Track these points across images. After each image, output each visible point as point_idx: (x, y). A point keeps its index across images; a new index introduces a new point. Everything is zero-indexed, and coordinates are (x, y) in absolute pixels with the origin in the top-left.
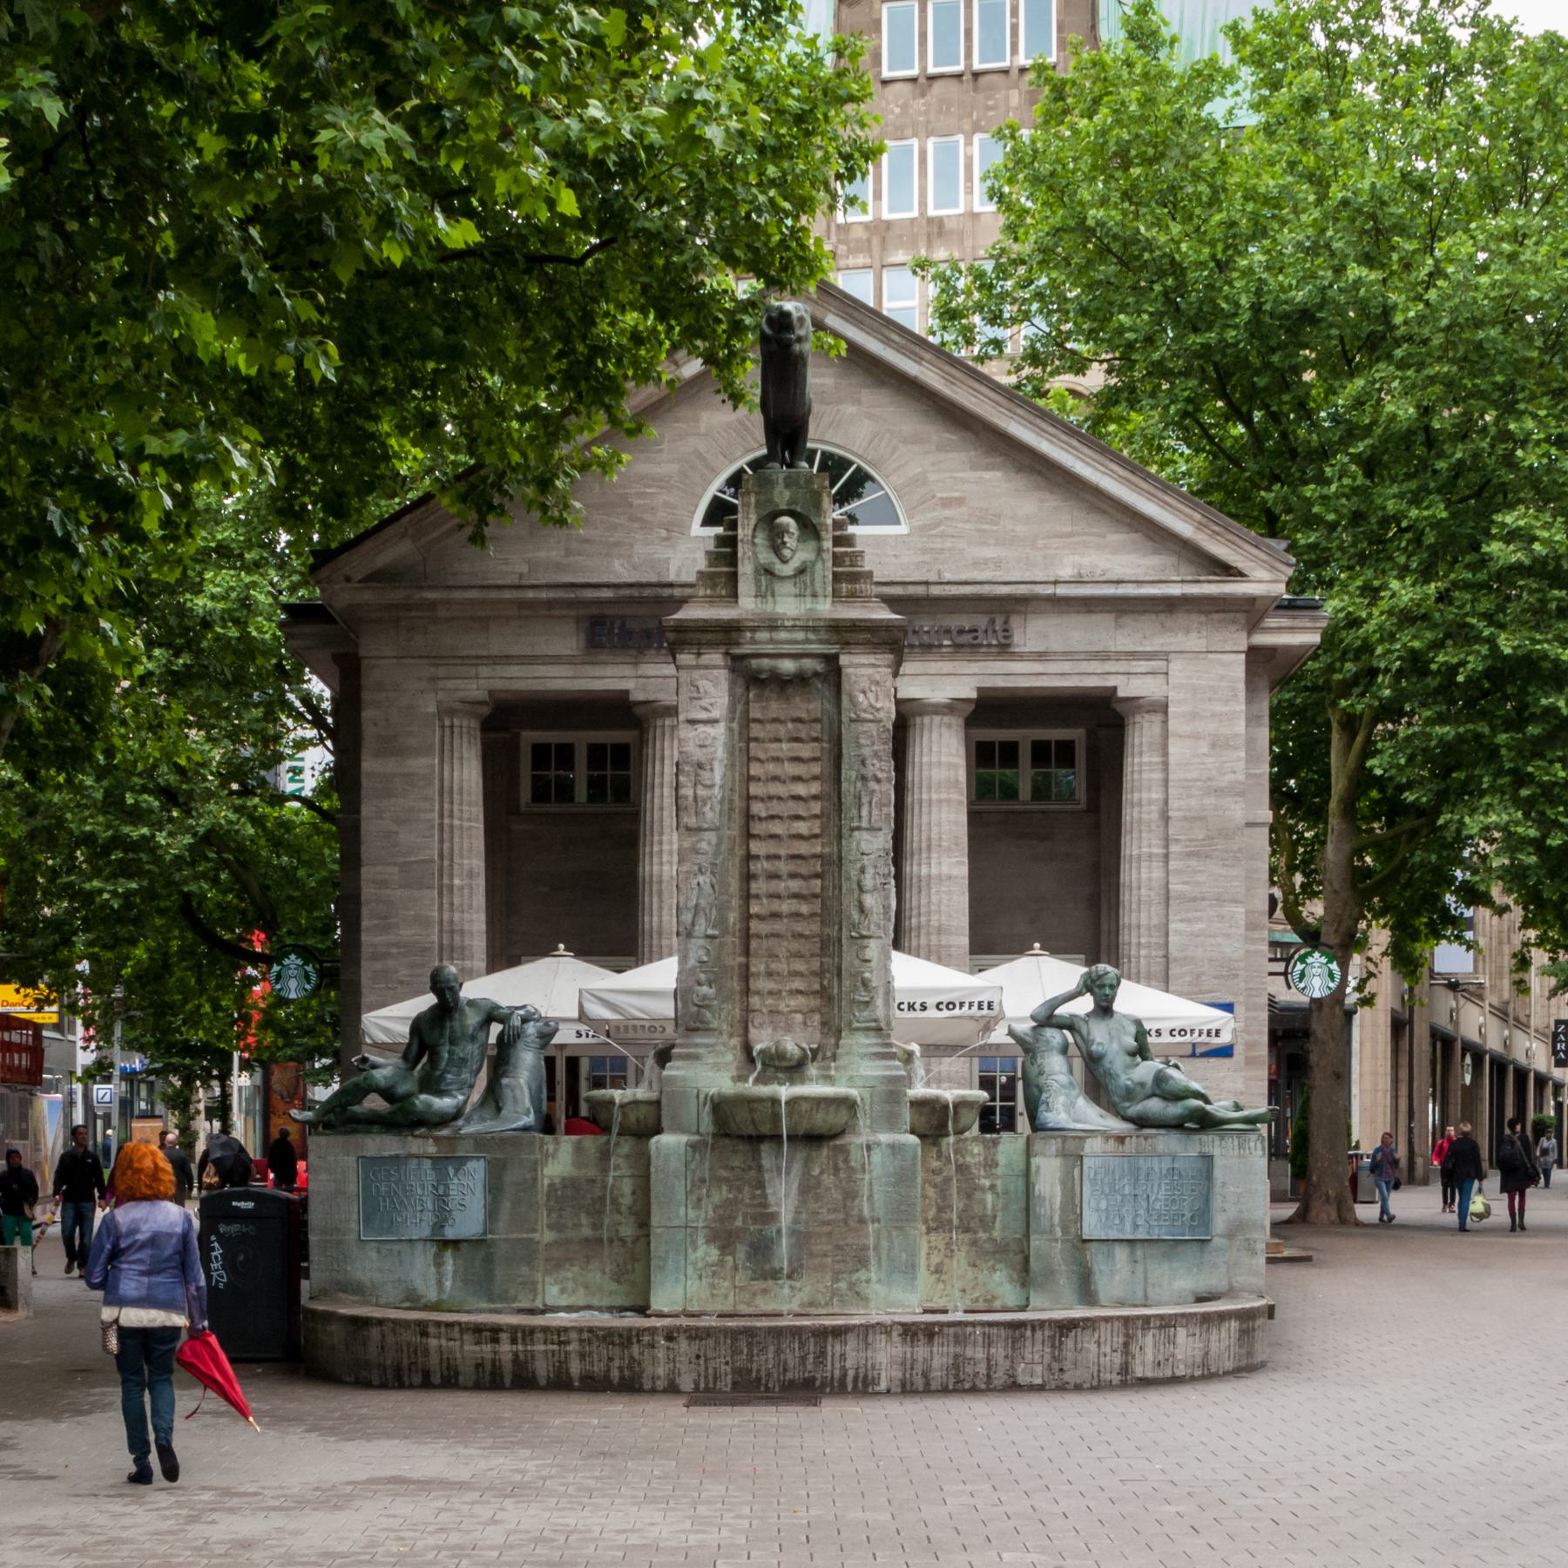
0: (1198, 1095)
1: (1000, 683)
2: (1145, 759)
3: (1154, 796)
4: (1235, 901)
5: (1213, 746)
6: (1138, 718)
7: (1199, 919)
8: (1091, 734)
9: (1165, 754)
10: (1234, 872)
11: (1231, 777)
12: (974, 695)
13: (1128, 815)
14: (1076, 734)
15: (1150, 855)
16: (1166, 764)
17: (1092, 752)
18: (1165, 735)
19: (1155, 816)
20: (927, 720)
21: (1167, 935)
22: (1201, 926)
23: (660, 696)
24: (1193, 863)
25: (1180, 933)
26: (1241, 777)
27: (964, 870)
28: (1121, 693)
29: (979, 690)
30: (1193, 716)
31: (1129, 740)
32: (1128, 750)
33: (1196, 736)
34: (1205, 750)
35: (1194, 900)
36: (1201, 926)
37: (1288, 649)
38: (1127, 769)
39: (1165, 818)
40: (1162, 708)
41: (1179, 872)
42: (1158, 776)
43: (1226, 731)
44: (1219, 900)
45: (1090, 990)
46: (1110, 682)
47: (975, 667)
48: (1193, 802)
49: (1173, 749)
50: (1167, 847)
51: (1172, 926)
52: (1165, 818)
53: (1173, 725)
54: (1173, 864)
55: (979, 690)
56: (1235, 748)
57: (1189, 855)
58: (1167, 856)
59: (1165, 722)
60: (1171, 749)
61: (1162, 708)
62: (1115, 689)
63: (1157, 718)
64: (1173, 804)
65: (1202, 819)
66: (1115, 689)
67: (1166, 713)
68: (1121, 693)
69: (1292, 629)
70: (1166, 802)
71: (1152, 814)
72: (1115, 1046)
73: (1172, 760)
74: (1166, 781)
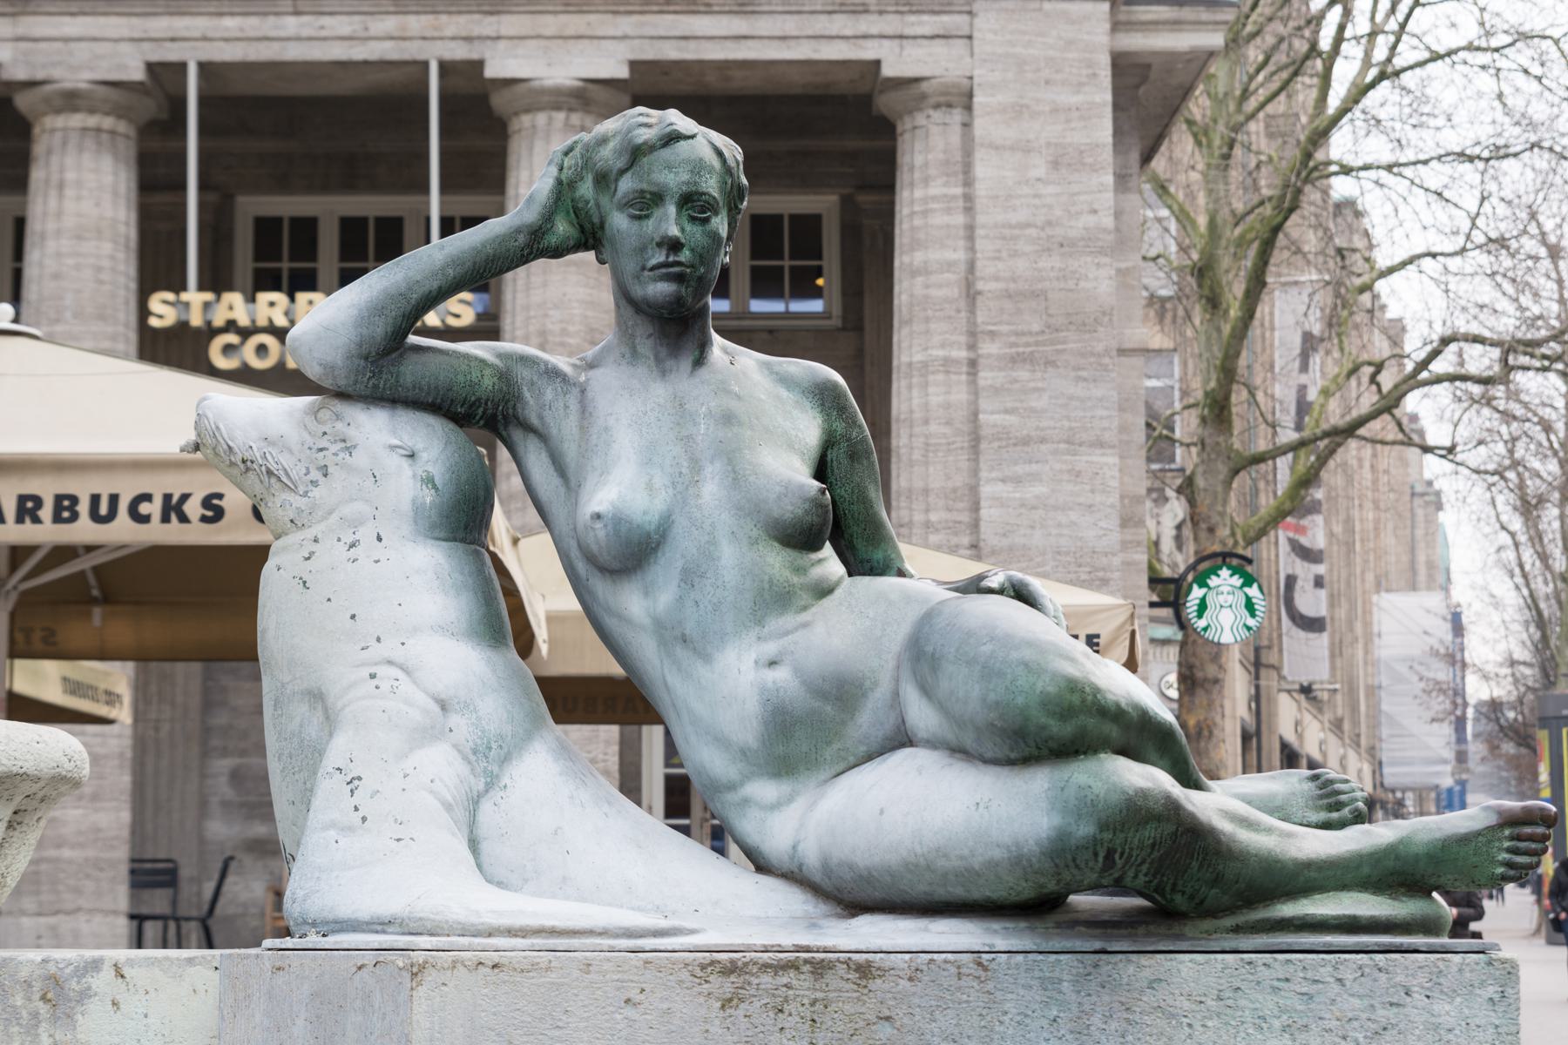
0: (1139, 736)
1: (671, 52)
2: (936, 189)
3: (950, 255)
4: (1100, 444)
5: (1055, 164)
6: (920, 119)
7: (1035, 478)
8: (847, 203)
9: (968, 182)
10: (1098, 392)
11: (1090, 220)
12: (623, 73)
13: (906, 291)
14: (822, 203)
15: (947, 362)
16: (968, 198)
17: (851, 232)
19: (954, 292)
20: (541, 118)
21: (976, 507)
22: (1040, 489)
23: (56, 73)
24: (1023, 374)
25: (1000, 502)
26: (1108, 221)
28: (888, 71)
29: (634, 65)
30: (1019, 111)
31: (903, 159)
32: (903, 177)
33: (1025, 148)
34: (1039, 168)
35: (1026, 441)
36: (1040, 489)
37: (1172, 57)
38: (903, 211)
39: (971, 295)
40: (962, 99)
41: (997, 391)
42: (959, 219)
43: (1078, 138)
44: (1072, 442)
45: (590, 237)
46: (867, 52)
47: (626, 24)
48: (1021, 265)
49: (984, 169)
50: (972, 347)
51: (986, 490)
52: (971, 295)
53: (980, 126)
54: (986, 377)
55: (634, 65)
56: (1094, 168)
57: (1015, 360)
58: (973, 363)
59: (967, 125)
60: (980, 170)
61: (962, 99)
62: (877, 64)
63: (957, 116)
64: (985, 267)
65: (1035, 295)
66: (877, 64)
67: (969, 108)
68: (888, 71)
69: (1176, 25)
70: (971, 266)
71: (947, 288)
72: (711, 491)
73: (981, 190)
74: (970, 229)
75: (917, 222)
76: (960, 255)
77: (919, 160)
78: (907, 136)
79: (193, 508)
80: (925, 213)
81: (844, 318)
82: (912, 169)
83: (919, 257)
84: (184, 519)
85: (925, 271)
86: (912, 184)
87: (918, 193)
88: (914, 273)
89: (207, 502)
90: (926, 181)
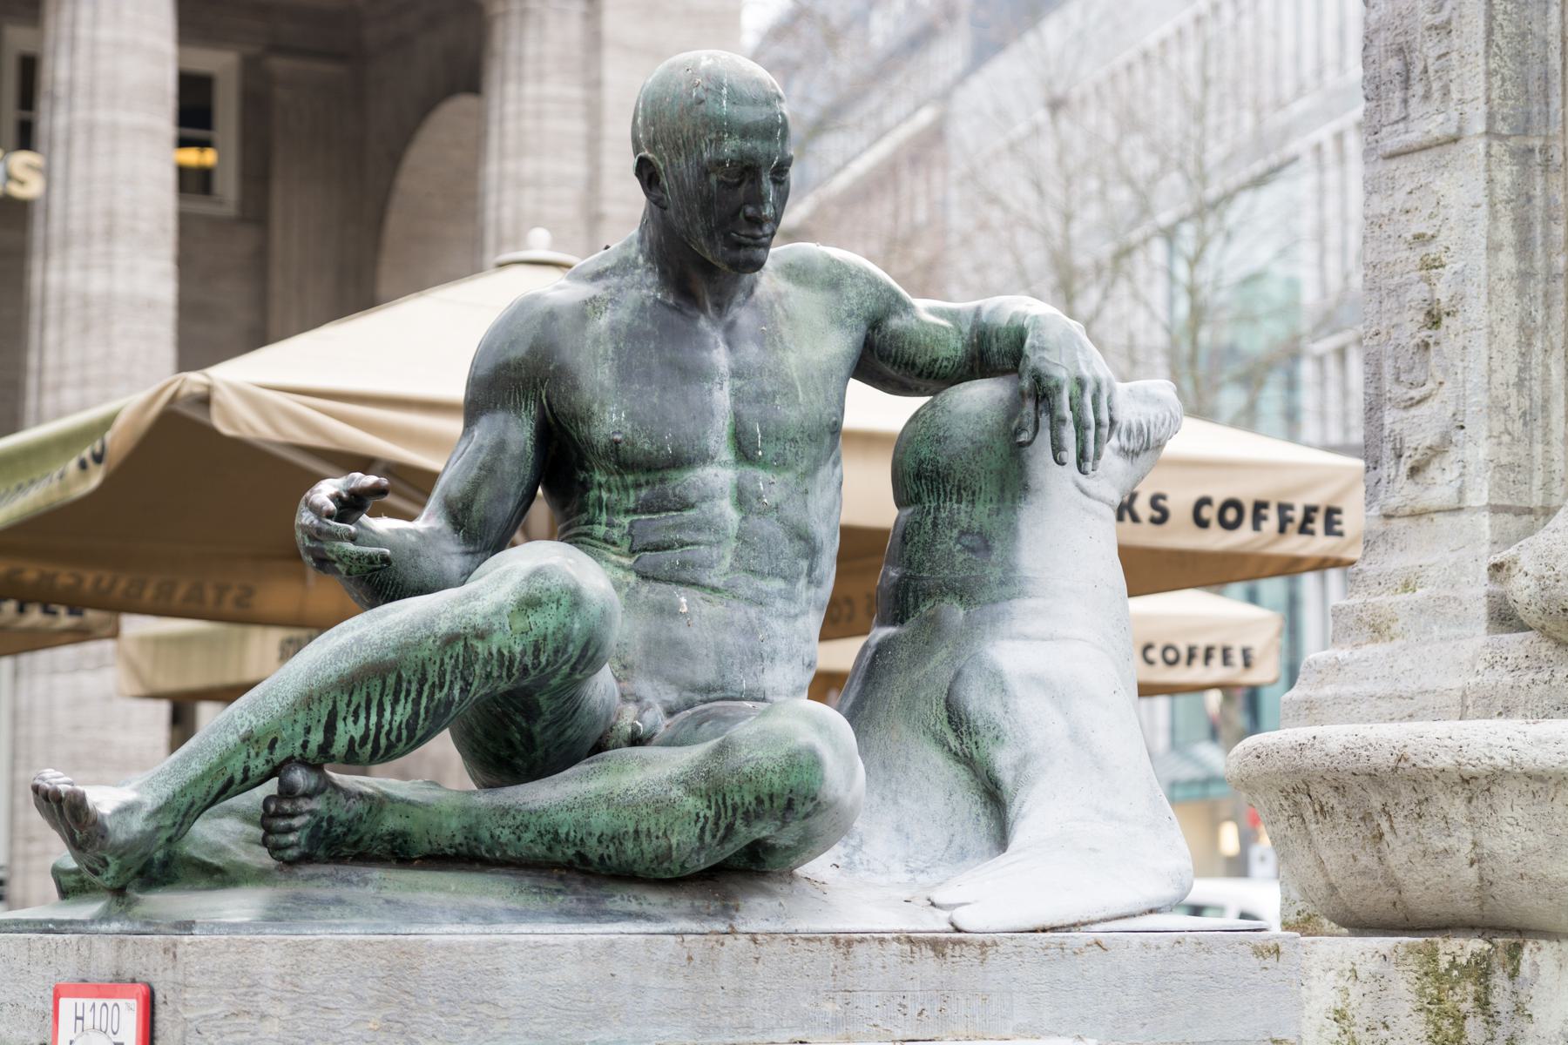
2: (552, 88)
17: (255, 103)
18: (594, 41)
27: (167, 291)
42: (577, 127)
75: (528, 124)
76: (575, 167)
77: (531, 50)
78: (514, 20)
79: (1143, 507)
80: (539, 115)
81: (243, 204)
82: (520, 60)
83: (529, 166)
84: (1135, 519)
85: (537, 182)
86: (521, 79)
87: (530, 89)
88: (520, 183)
89: (1155, 501)
90: (540, 77)
